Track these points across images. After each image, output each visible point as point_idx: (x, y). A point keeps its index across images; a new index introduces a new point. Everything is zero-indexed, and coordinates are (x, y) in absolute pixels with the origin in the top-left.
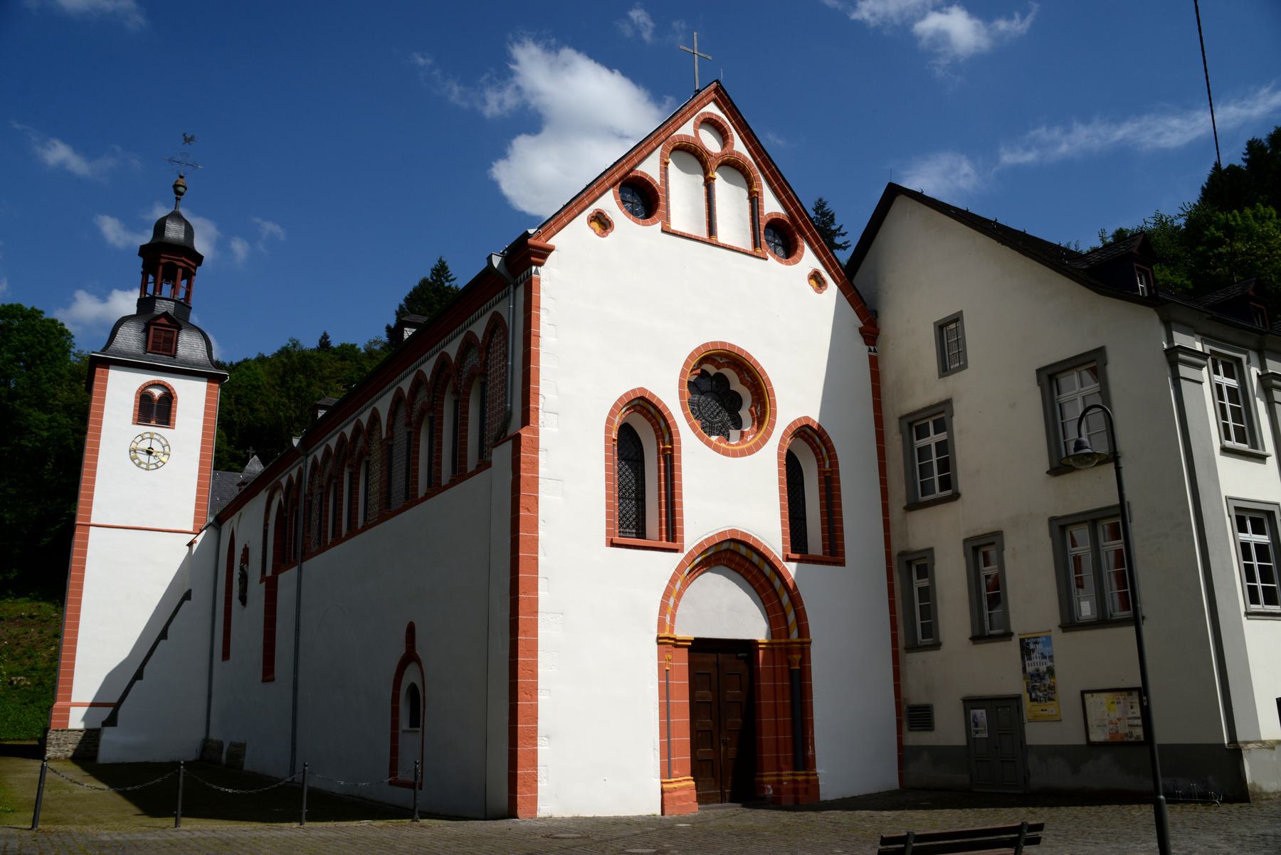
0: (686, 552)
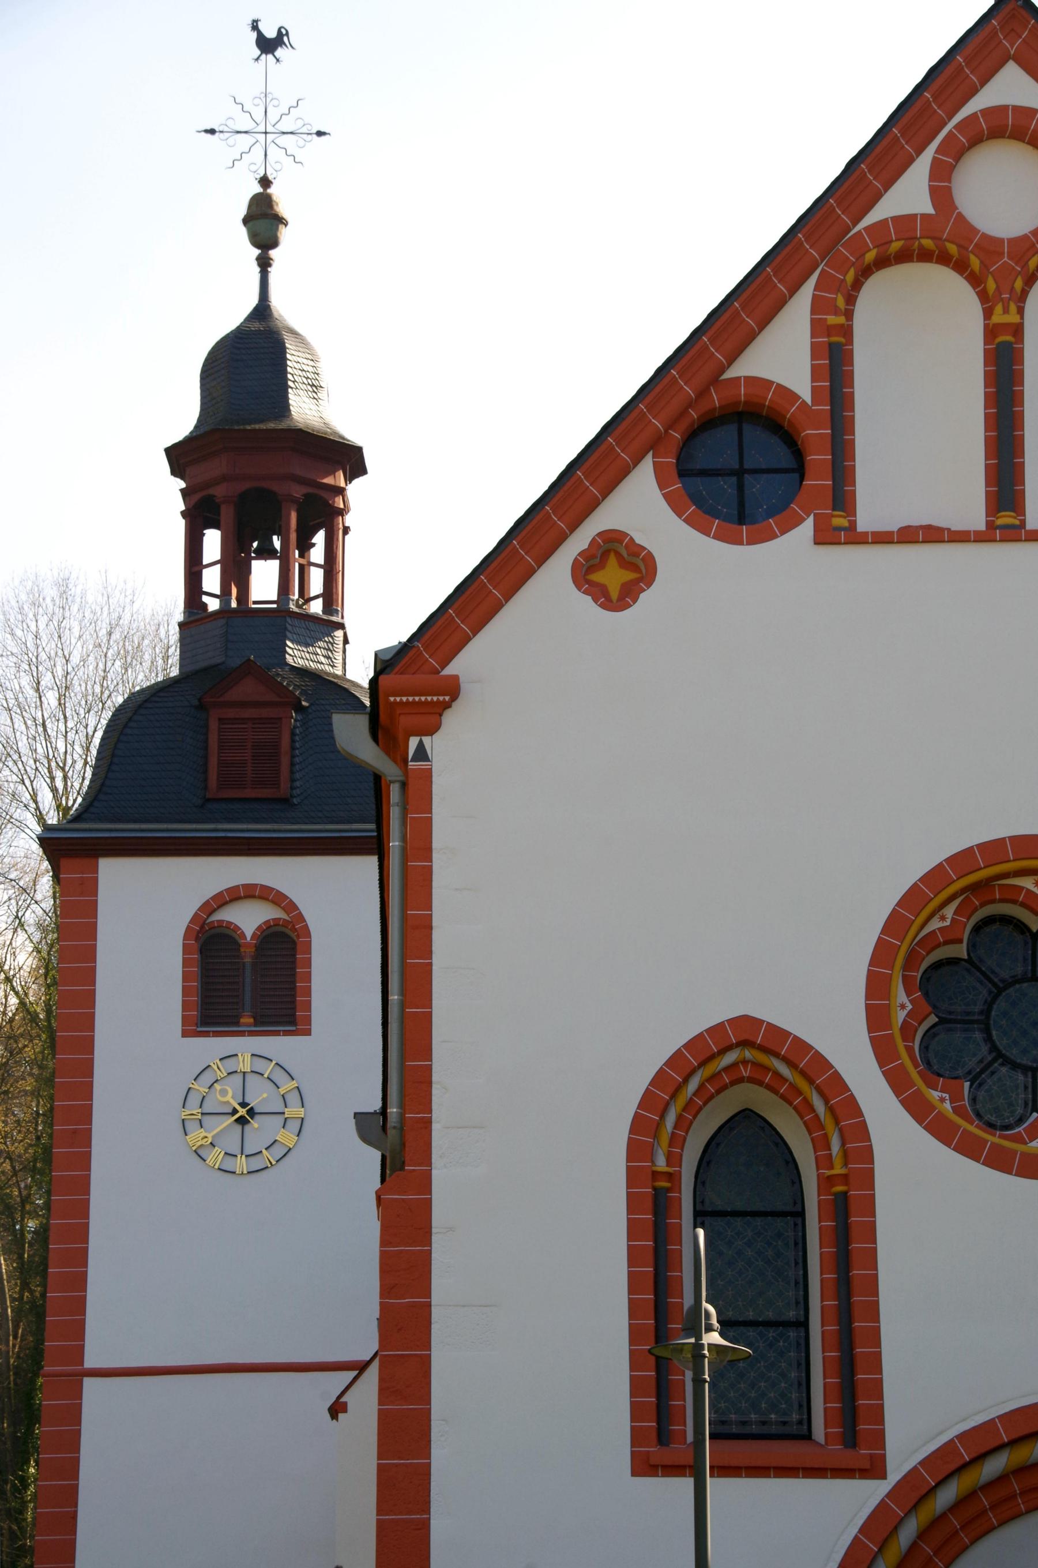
0: (894, 1476)
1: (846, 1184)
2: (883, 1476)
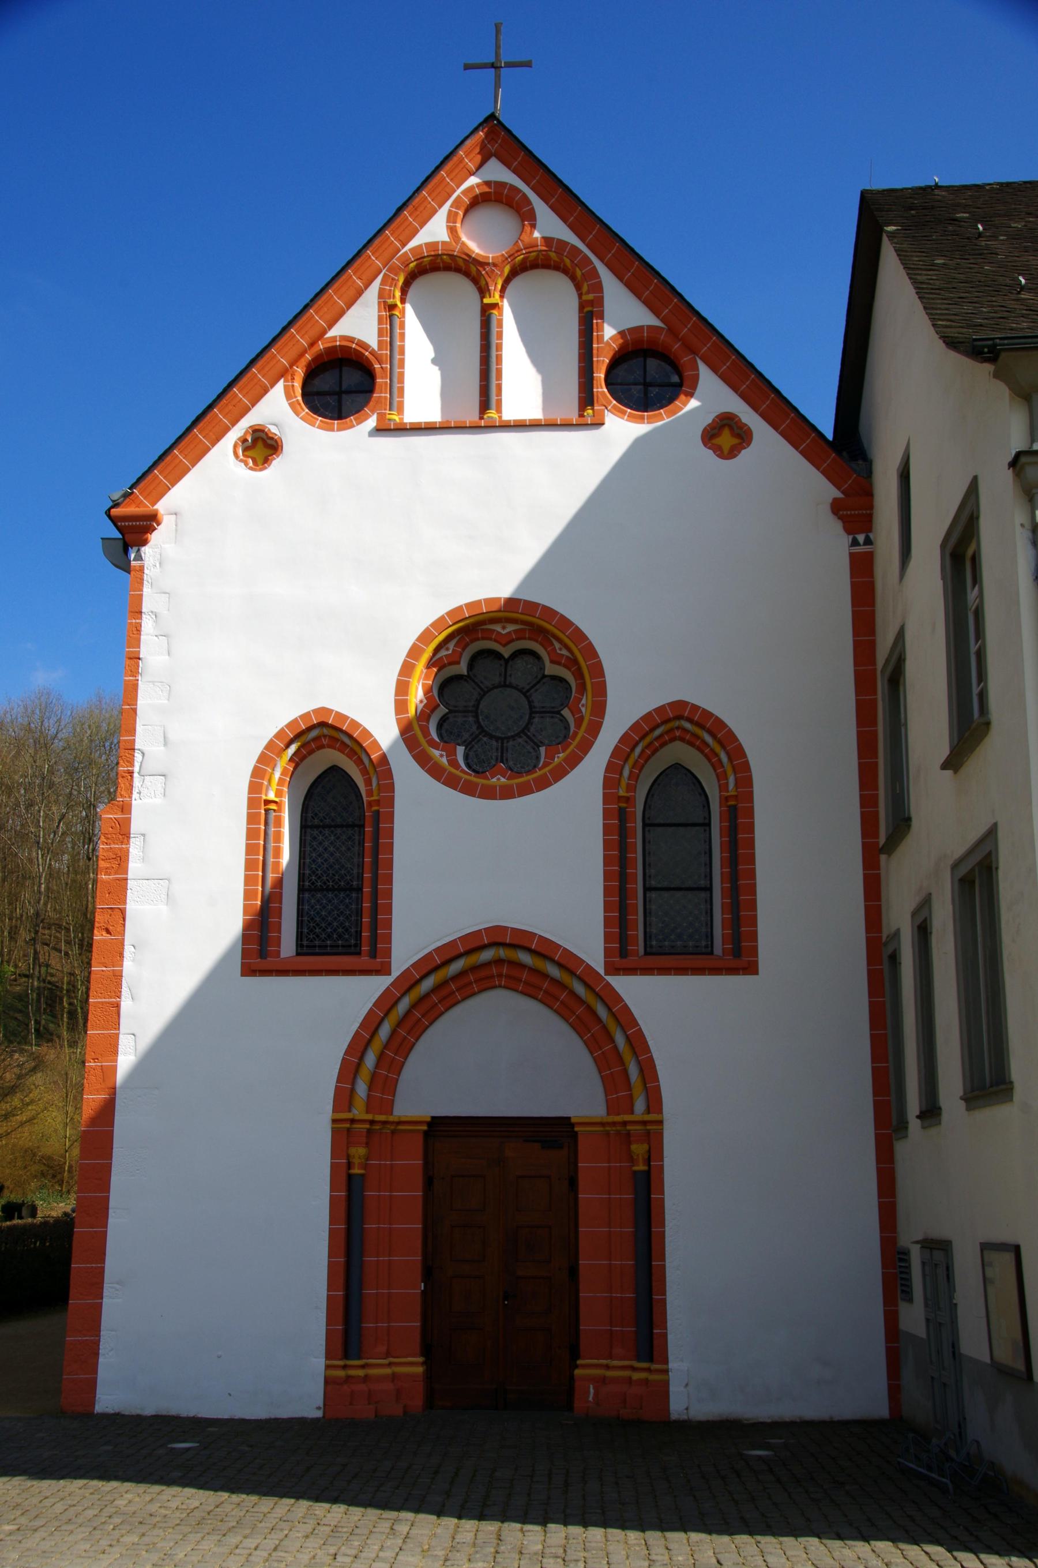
0: (396, 972)
1: (379, 805)
2: (389, 973)
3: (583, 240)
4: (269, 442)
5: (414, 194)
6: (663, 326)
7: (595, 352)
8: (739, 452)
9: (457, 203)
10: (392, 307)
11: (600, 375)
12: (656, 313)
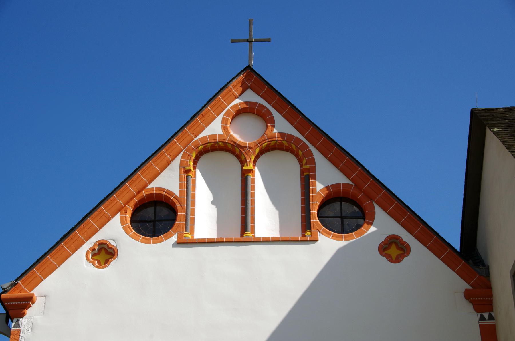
3: (303, 135)
4: (109, 250)
5: (202, 108)
6: (352, 183)
7: (311, 198)
8: (403, 259)
9: (228, 113)
10: (188, 171)
11: (314, 211)
12: (348, 176)
